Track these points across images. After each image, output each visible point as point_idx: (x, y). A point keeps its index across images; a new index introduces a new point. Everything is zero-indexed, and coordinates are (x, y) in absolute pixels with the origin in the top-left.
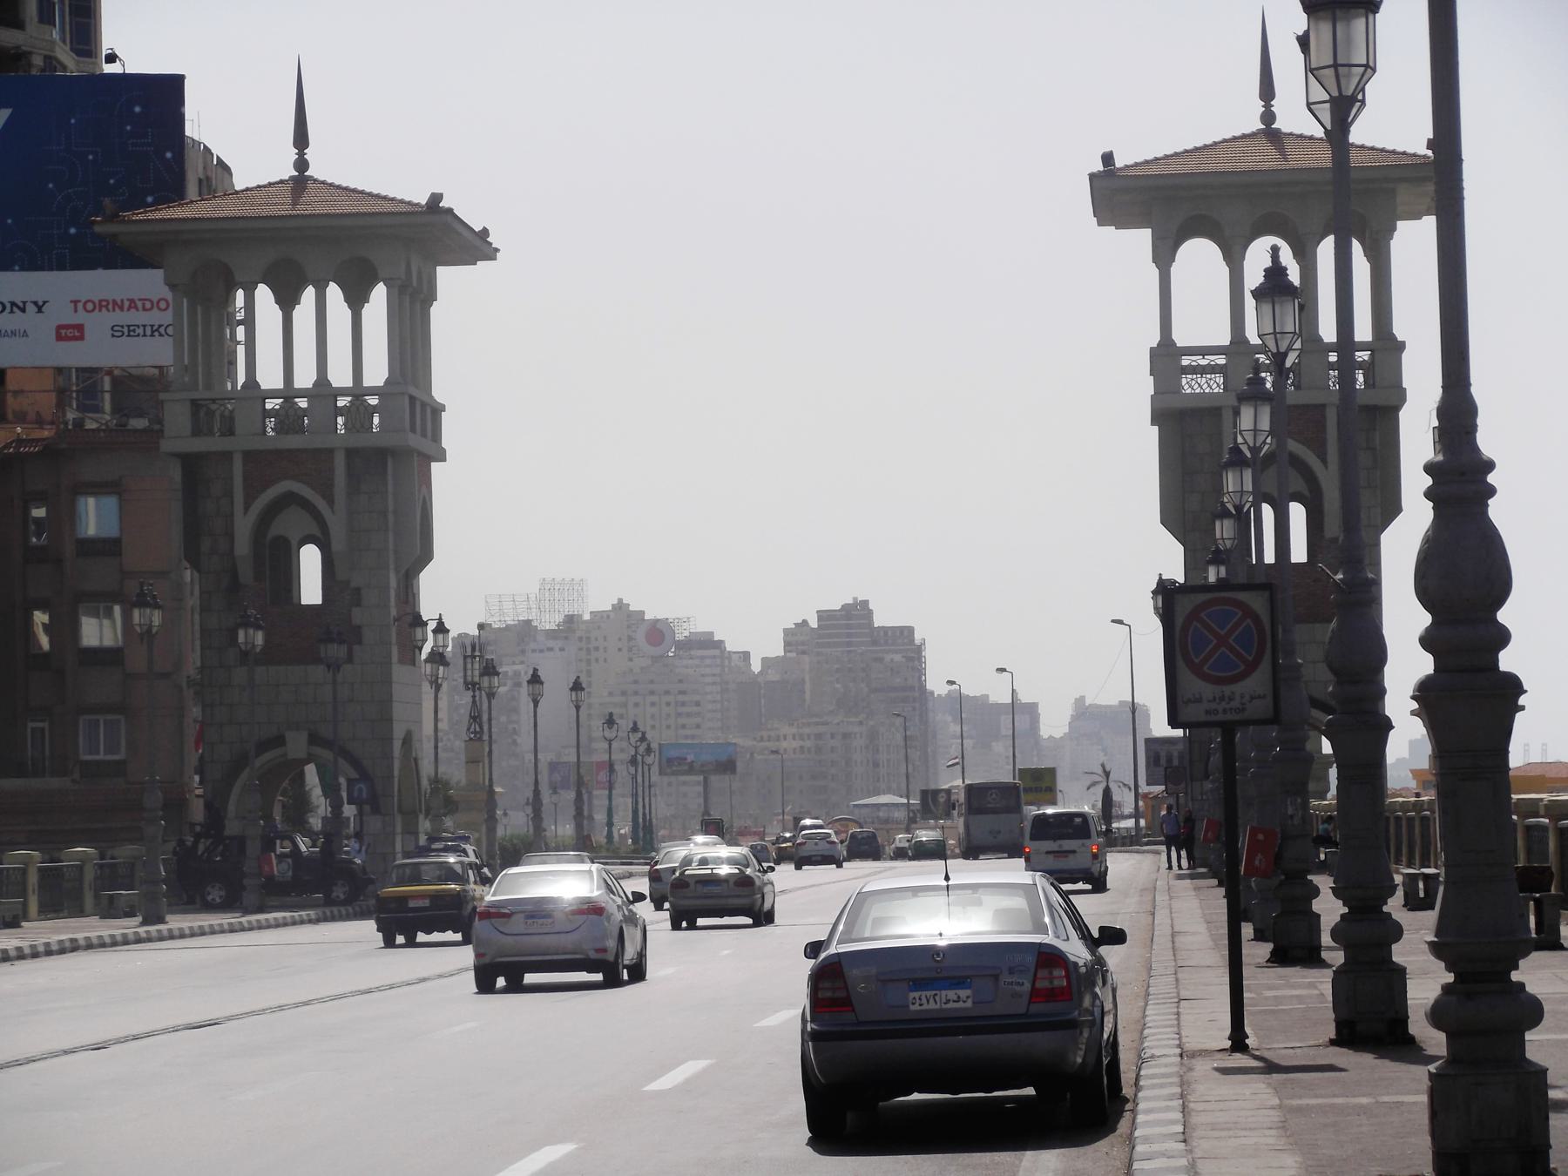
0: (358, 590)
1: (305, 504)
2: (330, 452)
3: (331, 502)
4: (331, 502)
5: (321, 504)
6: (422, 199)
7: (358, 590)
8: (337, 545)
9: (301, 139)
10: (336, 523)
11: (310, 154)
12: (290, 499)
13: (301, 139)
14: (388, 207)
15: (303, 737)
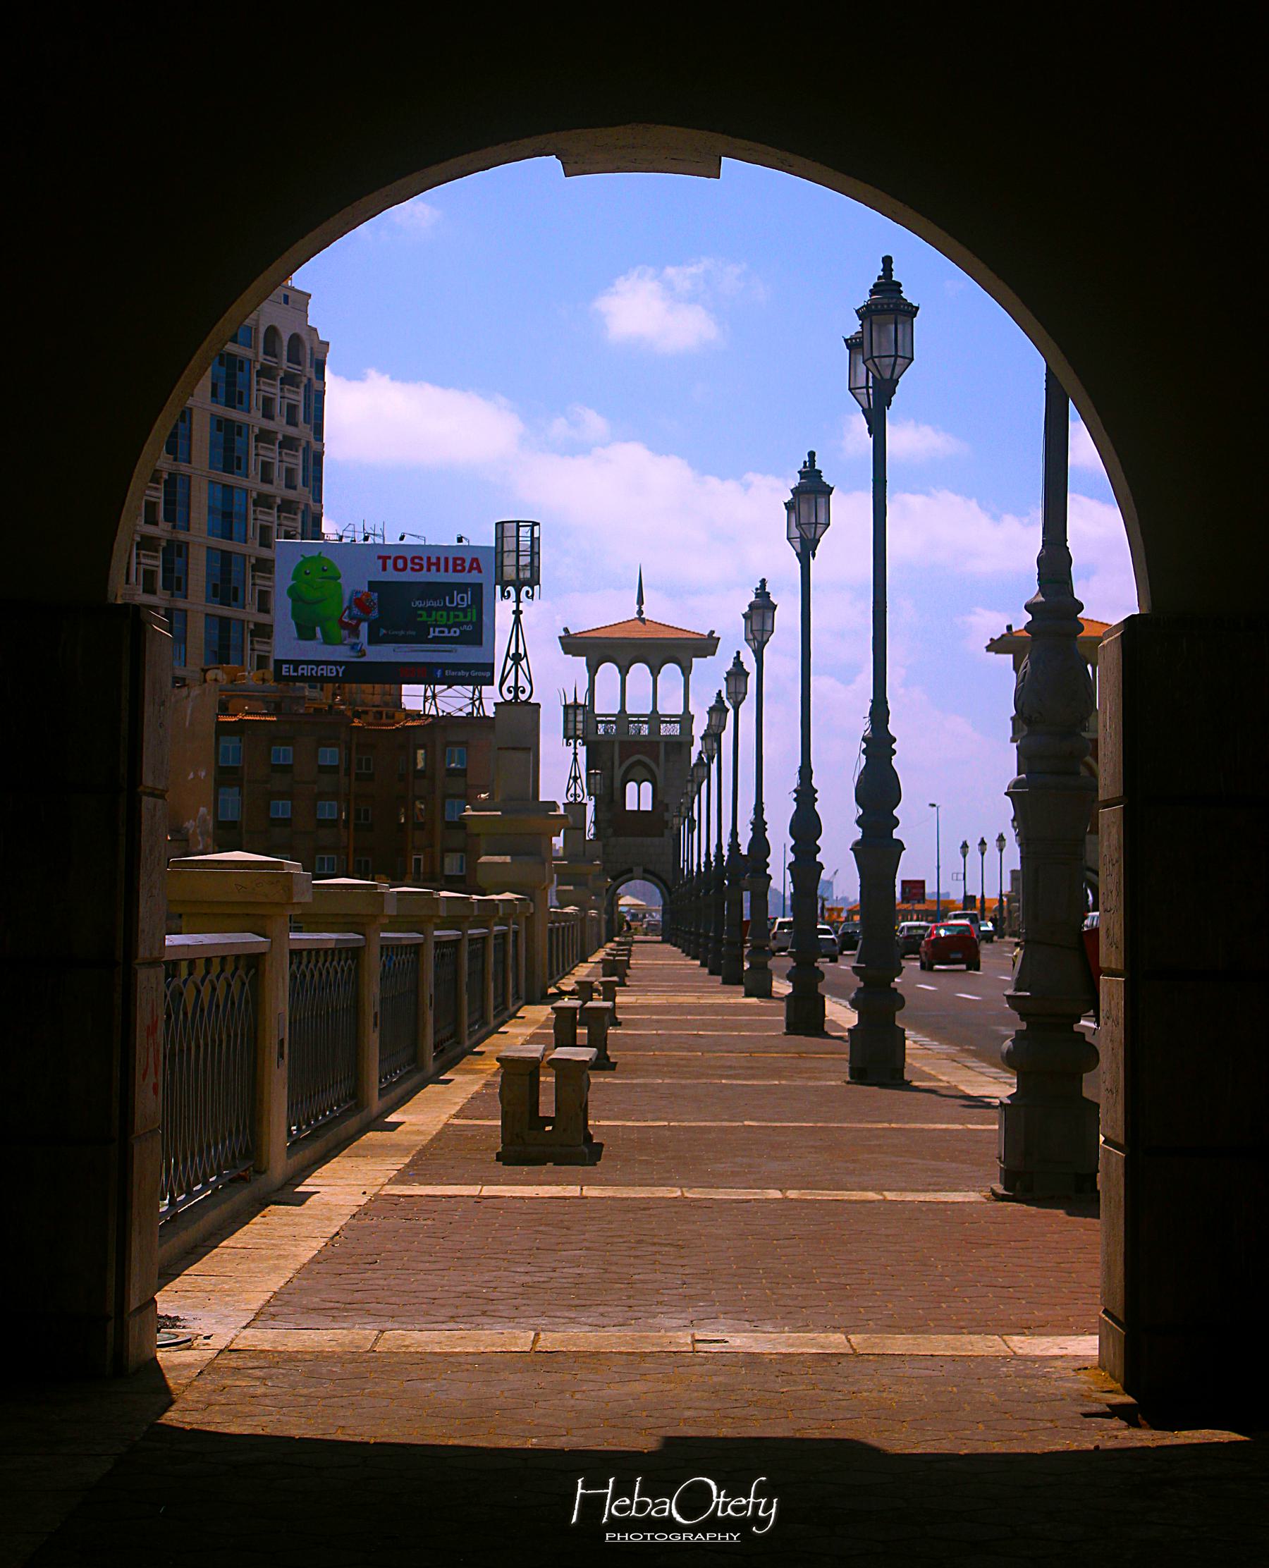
0: (667, 805)
1: (645, 765)
2: (658, 743)
3: (658, 765)
4: (658, 765)
5: (653, 766)
6: (706, 633)
7: (667, 805)
8: (659, 785)
9: (640, 601)
10: (659, 774)
11: (643, 608)
12: (639, 762)
13: (640, 601)
14: (680, 635)
15: (641, 869)
